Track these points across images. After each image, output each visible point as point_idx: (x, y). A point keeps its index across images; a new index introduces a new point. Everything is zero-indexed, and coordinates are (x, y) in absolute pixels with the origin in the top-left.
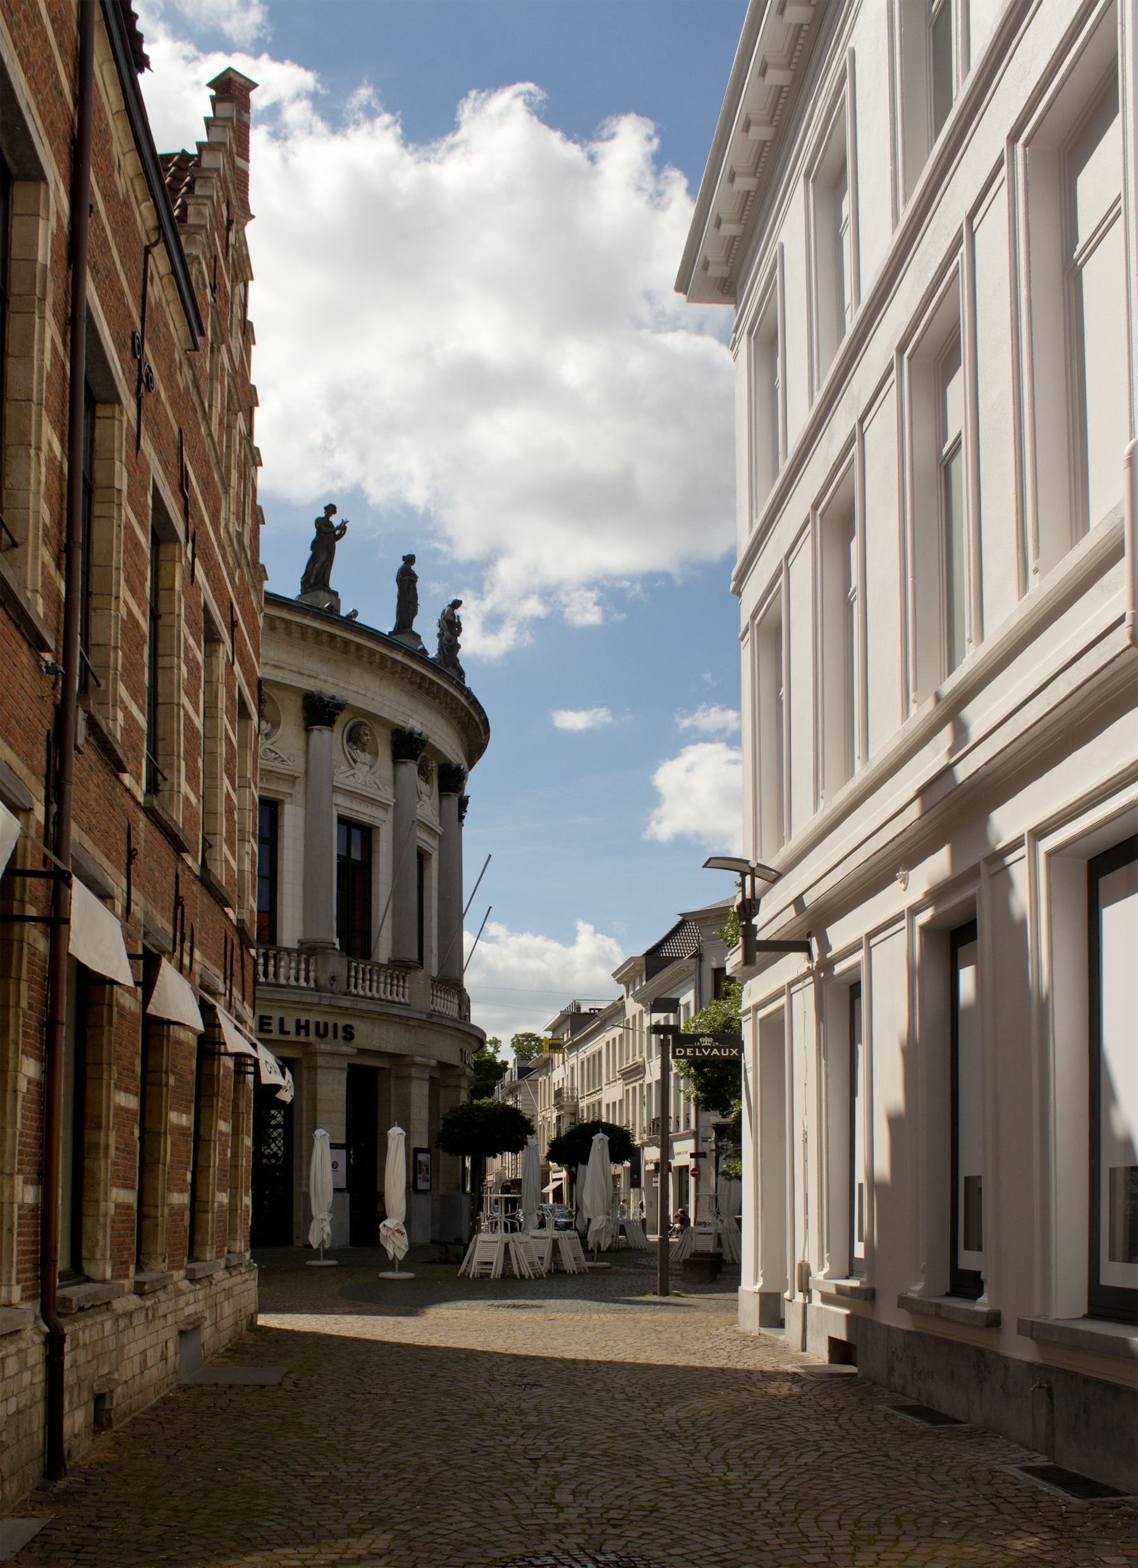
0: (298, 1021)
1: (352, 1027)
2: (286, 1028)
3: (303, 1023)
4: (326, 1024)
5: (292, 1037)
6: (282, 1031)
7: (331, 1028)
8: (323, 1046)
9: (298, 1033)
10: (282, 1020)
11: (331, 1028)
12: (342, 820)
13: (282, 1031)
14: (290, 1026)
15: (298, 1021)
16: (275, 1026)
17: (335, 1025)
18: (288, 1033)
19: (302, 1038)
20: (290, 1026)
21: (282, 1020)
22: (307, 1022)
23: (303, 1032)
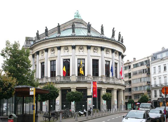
12: (105, 61)
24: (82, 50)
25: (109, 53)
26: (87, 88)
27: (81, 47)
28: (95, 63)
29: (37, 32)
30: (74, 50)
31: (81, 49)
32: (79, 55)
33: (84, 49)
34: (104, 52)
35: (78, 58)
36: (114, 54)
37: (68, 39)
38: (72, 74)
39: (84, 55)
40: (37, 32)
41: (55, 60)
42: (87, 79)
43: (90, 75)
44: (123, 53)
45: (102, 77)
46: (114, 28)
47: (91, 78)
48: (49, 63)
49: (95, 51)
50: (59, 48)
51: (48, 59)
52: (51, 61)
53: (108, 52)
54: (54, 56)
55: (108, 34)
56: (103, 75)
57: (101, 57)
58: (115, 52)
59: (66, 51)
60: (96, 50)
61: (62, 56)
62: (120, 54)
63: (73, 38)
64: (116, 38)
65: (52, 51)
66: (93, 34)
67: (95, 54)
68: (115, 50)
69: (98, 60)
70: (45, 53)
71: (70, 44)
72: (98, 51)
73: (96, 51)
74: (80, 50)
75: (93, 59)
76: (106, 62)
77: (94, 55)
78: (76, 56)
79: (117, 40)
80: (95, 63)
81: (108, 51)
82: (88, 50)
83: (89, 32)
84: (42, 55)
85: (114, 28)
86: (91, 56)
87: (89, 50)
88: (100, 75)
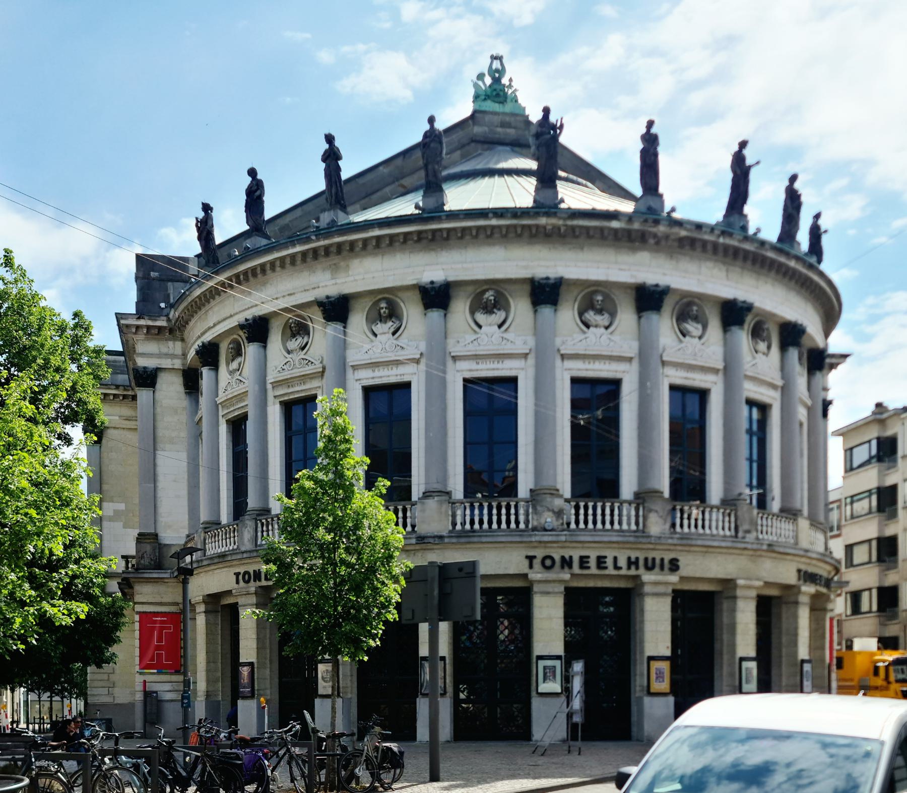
0: (629, 558)
1: (677, 560)
2: (619, 565)
3: (633, 559)
4: (654, 559)
5: (624, 572)
6: (616, 567)
7: (658, 562)
8: (647, 577)
9: (629, 568)
10: (615, 559)
11: (658, 562)
13: (616, 567)
14: (622, 562)
15: (629, 558)
16: (609, 562)
17: (662, 560)
18: (620, 568)
19: (633, 572)
20: (622, 562)
21: (615, 559)
22: (637, 559)
23: (633, 567)
24: (500, 316)
25: (705, 327)
26: (532, 583)
27: (490, 298)
28: (596, 402)
29: (201, 215)
30: (435, 315)
31: (489, 309)
32: (472, 349)
33: (507, 309)
34: (664, 326)
35: (468, 375)
36: (742, 337)
37: (392, 238)
38: (422, 490)
39: (508, 349)
40: (201, 215)
41: (314, 397)
42: (527, 522)
43: (555, 492)
44: (812, 323)
45: (642, 498)
46: (743, 145)
47: (559, 513)
48: (275, 414)
49: (590, 316)
50: (337, 310)
51: (271, 394)
52: (288, 407)
53: (693, 328)
54: (309, 369)
55: (693, 192)
56: (654, 485)
57: (635, 365)
58: (750, 321)
59: (379, 328)
60: (600, 312)
61: (355, 368)
62: (791, 334)
63: (435, 230)
64: (763, 217)
65: (294, 336)
66: (574, 196)
67: (597, 339)
68: (748, 308)
69: (614, 385)
70: (251, 350)
71: (410, 280)
72: (613, 315)
73: (603, 319)
74: (481, 317)
75: (575, 381)
76: (679, 395)
77: (580, 349)
78: (450, 362)
79: (771, 232)
80: (596, 402)
81: (696, 319)
82: (536, 311)
83: (546, 179)
84: (234, 365)
85: (743, 145)
86: (563, 357)
87: (546, 311)
88: (628, 486)
